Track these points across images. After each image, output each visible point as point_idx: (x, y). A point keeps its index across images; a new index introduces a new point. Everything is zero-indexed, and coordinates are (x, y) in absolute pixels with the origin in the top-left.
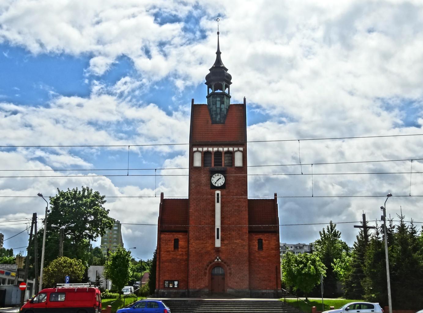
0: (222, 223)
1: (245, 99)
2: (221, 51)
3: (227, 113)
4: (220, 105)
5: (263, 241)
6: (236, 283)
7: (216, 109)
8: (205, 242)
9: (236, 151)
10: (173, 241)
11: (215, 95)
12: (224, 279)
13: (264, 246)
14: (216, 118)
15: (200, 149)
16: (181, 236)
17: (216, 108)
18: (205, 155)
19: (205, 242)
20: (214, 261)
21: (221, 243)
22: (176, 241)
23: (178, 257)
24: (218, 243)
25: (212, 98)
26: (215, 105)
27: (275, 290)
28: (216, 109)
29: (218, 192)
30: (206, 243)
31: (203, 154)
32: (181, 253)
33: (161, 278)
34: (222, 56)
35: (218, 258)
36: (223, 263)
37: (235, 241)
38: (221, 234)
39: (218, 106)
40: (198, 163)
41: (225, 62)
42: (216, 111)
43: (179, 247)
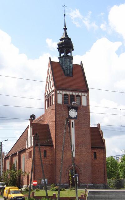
1: (81, 62)
5: (97, 153)
6: (85, 179)
8: (66, 153)
9: (83, 96)
10: (43, 152)
13: (97, 157)
15: (61, 92)
16: (48, 149)
18: (65, 97)
19: (66, 153)
21: (75, 154)
23: (47, 163)
25: (65, 59)
27: (104, 184)
29: (73, 121)
30: (66, 154)
31: (63, 95)
32: (48, 160)
37: (84, 153)
38: (75, 148)
39: (68, 64)
41: (69, 36)
43: (47, 156)
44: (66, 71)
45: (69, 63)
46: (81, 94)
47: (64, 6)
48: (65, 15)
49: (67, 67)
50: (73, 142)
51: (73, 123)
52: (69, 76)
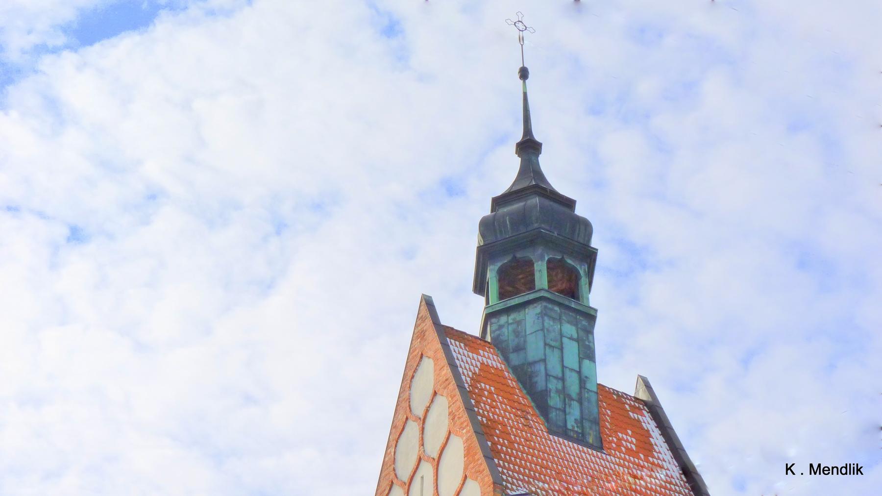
25: (542, 315)
42: (563, 379)
44: (559, 405)
45: (571, 350)
47: (520, 25)
48: (524, 74)
49: (558, 371)
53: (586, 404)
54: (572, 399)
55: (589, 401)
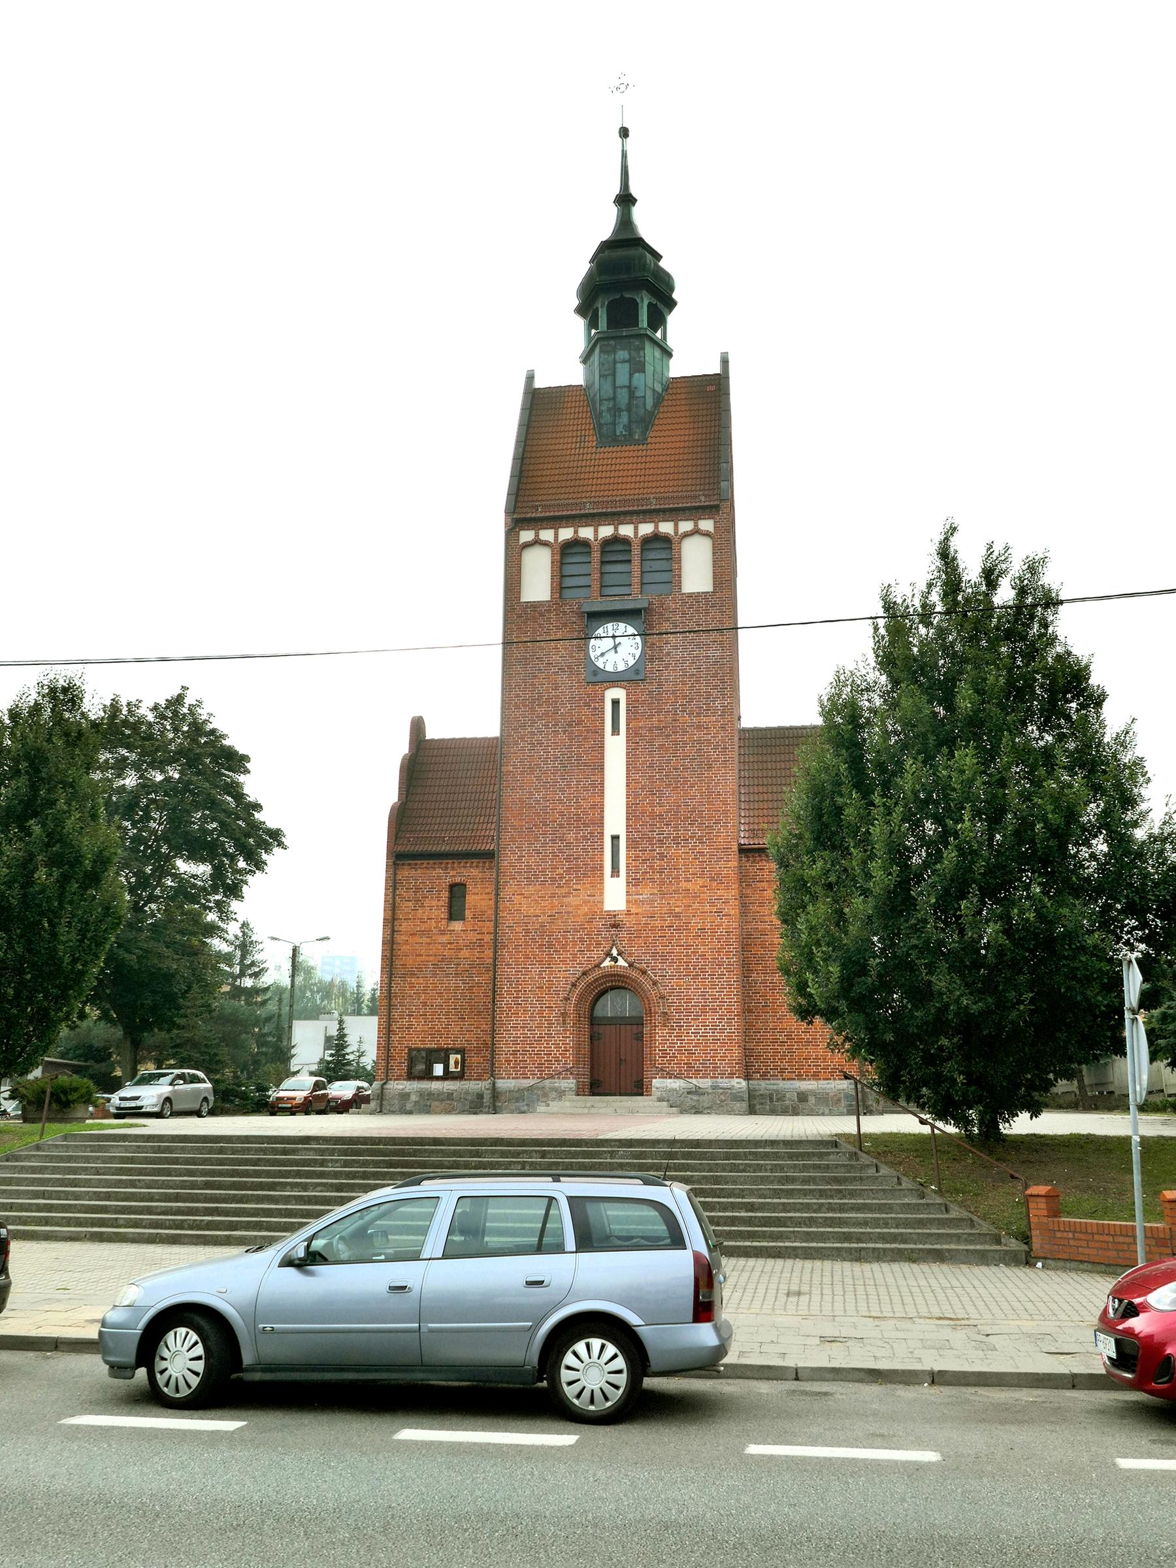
0: (633, 814)
1: (725, 362)
2: (634, 191)
3: (656, 405)
4: (627, 375)
7: (615, 393)
9: (687, 535)
10: (445, 895)
11: (612, 342)
12: (639, 1037)
14: (614, 424)
15: (547, 535)
16: (474, 872)
17: (615, 387)
20: (598, 966)
22: (457, 892)
24: (615, 895)
26: (610, 379)
28: (615, 393)
29: (619, 693)
33: (395, 1038)
34: (638, 214)
35: (614, 952)
36: (634, 974)
37: (683, 885)
39: (622, 378)
40: (538, 585)
42: (614, 398)
45: (623, 371)
46: (676, 526)
47: (623, 87)
48: (624, 133)
50: (615, 820)
51: (616, 703)
52: (629, 440)
53: (634, 410)
54: (620, 410)
55: (637, 406)
